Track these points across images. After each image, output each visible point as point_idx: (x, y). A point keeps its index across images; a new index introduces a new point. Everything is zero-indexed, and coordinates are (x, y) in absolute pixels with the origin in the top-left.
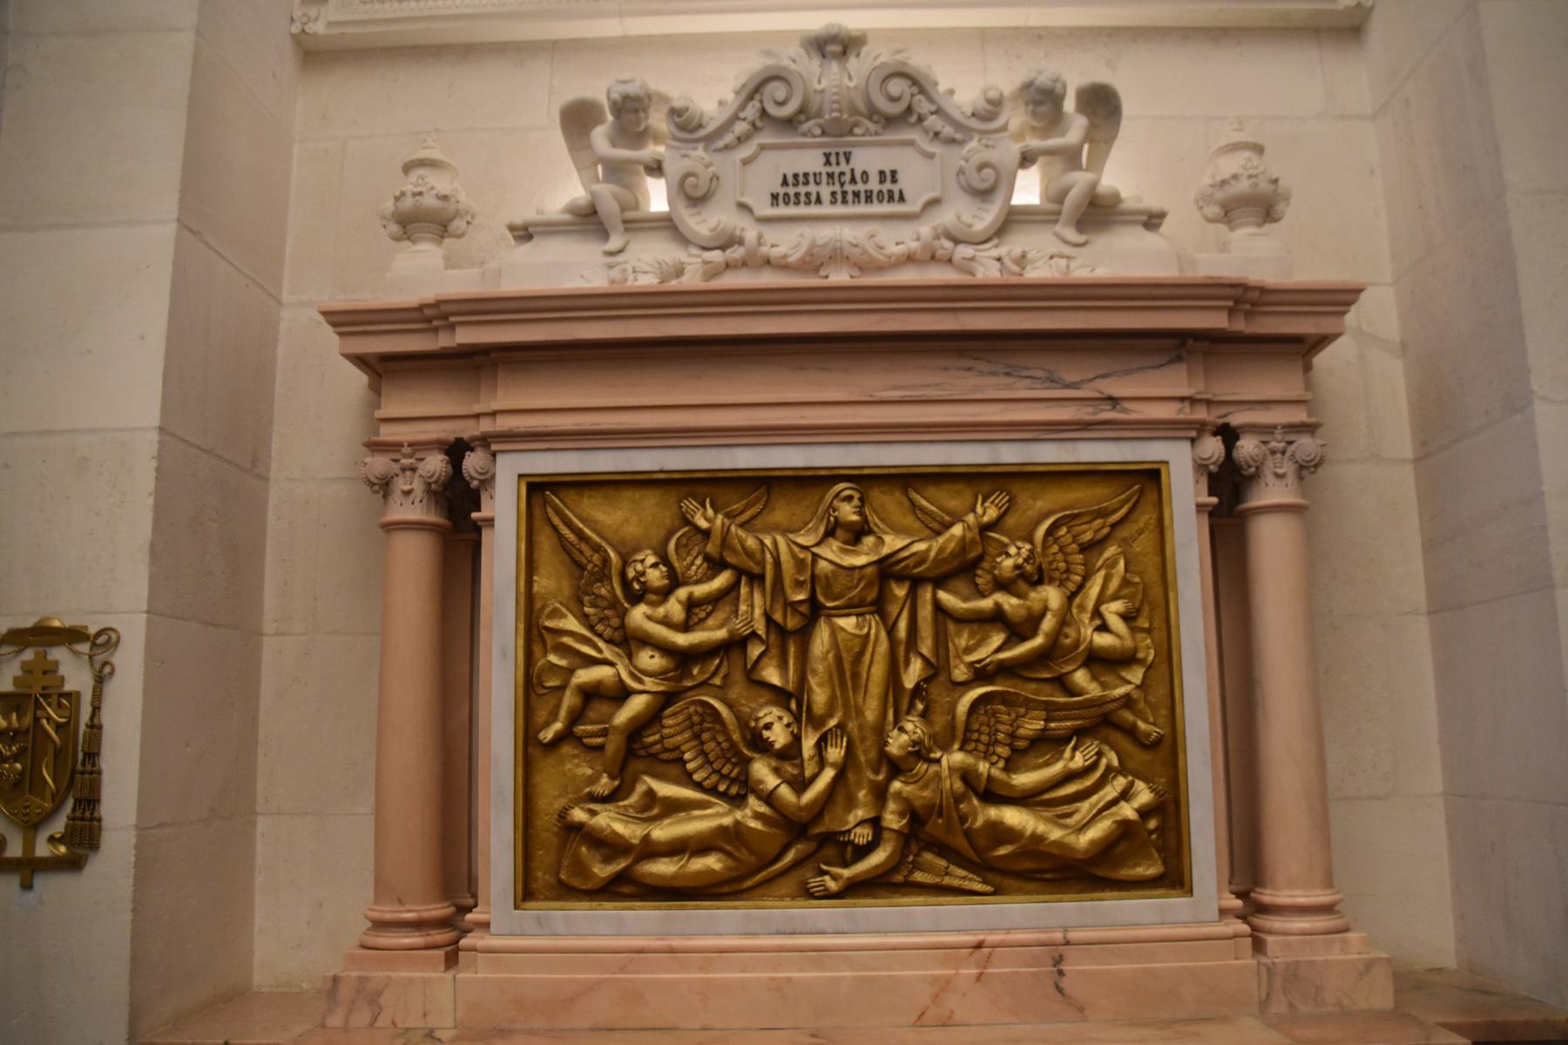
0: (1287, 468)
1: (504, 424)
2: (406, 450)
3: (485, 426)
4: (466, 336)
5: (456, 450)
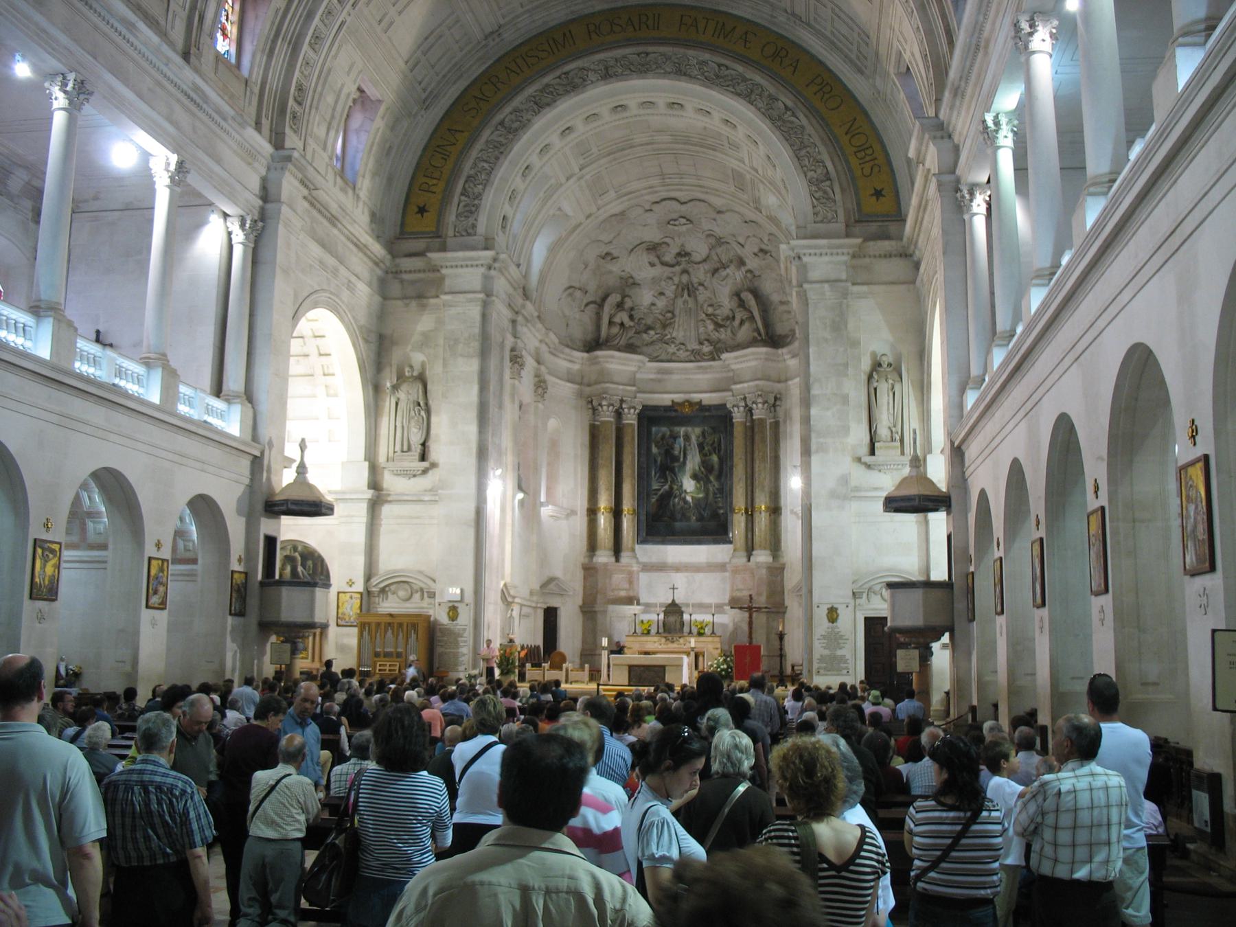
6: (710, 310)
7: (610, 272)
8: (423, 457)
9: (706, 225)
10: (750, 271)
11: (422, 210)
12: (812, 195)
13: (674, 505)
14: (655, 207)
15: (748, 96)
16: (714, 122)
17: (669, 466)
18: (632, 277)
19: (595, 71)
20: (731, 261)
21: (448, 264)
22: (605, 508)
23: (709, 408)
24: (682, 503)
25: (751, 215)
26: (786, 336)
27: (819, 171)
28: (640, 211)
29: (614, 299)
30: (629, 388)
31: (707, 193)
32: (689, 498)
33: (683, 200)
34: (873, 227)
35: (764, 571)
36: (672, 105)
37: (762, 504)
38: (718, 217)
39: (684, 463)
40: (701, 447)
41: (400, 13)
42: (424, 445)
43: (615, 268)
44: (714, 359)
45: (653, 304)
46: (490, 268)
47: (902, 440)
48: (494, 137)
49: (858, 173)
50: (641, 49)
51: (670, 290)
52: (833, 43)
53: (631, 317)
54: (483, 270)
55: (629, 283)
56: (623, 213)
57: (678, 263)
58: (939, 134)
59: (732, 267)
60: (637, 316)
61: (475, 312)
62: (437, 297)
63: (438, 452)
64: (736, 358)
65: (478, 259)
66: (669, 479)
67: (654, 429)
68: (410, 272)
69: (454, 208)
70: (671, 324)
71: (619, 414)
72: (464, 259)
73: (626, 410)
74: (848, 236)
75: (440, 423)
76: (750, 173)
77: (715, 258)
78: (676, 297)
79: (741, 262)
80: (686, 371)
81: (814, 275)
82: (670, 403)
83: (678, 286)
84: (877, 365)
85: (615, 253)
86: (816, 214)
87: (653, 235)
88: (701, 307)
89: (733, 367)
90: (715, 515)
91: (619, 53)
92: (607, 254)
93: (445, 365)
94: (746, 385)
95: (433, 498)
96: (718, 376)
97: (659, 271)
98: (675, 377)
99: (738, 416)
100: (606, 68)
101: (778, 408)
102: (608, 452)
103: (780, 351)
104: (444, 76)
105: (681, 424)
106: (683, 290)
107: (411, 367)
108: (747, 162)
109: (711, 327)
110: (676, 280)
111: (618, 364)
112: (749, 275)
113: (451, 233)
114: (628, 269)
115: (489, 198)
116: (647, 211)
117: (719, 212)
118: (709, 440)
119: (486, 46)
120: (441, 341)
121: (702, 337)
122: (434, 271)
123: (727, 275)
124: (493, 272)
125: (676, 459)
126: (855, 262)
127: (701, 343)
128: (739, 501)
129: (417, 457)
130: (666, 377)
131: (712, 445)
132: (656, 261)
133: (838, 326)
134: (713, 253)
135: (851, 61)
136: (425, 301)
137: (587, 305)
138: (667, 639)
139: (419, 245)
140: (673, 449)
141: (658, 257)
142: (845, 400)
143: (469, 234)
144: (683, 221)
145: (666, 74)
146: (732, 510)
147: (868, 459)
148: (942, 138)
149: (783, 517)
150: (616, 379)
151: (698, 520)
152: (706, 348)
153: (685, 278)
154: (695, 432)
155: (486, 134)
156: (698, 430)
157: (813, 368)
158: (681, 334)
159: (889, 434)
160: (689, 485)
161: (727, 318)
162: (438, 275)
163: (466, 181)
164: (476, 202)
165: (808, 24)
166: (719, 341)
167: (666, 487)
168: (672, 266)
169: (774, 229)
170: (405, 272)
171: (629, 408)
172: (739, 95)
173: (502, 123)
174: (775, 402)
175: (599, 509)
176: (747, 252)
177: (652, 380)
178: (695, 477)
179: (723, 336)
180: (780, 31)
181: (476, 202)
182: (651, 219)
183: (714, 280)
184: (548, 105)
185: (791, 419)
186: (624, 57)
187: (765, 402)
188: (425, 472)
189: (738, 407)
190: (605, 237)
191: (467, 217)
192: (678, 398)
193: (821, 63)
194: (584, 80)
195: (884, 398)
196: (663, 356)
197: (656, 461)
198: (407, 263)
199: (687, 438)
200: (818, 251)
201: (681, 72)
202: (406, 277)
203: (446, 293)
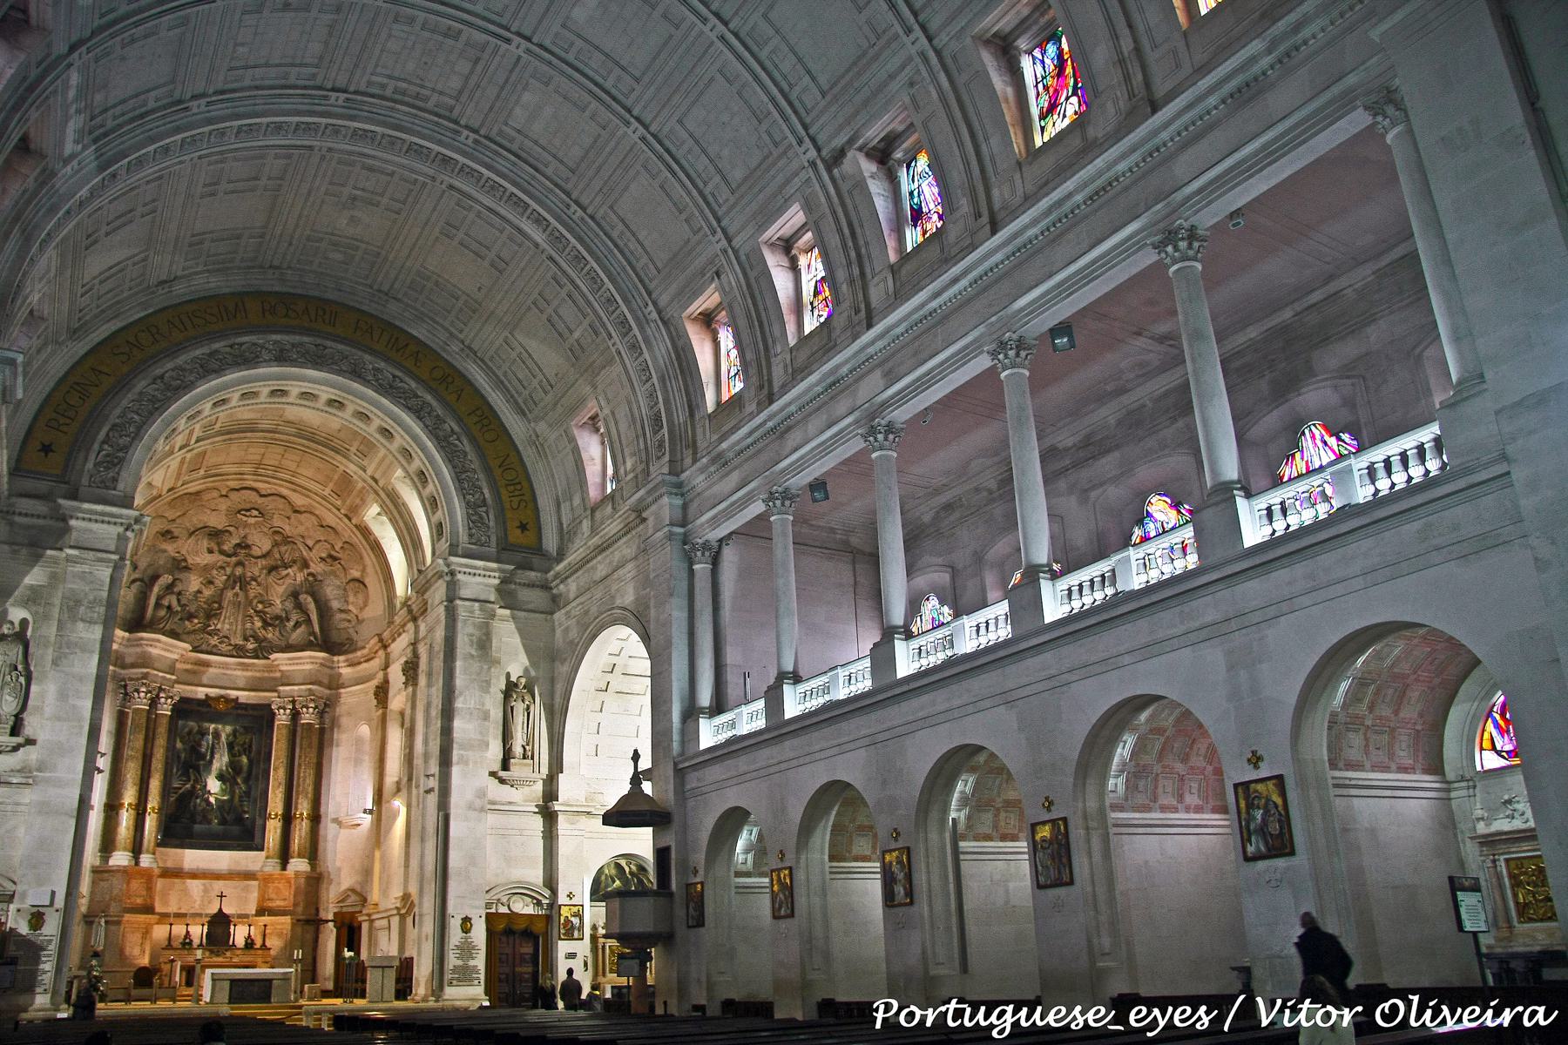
6: (260, 607)
7: (165, 551)
8: (15, 731)
9: (277, 522)
10: (310, 574)
11: (47, 449)
12: (469, 518)
13: (195, 806)
14: (233, 495)
15: (418, 412)
16: (371, 430)
17: (191, 763)
18: (185, 560)
19: (270, 351)
20: (294, 562)
21: (80, 515)
22: (130, 805)
23: (246, 706)
24: (204, 804)
25: (330, 519)
26: (343, 645)
27: (477, 496)
28: (215, 494)
29: (166, 579)
30: (168, 676)
31: (294, 491)
32: (212, 800)
33: (264, 493)
34: (519, 557)
35: (303, 880)
36: (331, 402)
37: (303, 807)
38: (293, 516)
39: (211, 762)
40: (231, 746)
41: (107, 234)
42: (16, 716)
43: (170, 548)
44: (258, 658)
45: (199, 592)
46: (127, 529)
47: (532, 758)
48: (150, 390)
49: (507, 506)
50: (319, 341)
51: (220, 580)
52: (502, 382)
53: (179, 600)
54: (121, 529)
55: (180, 566)
56: (198, 493)
57: (235, 554)
58: (674, 491)
59: (295, 568)
60: (184, 601)
61: (105, 573)
62: (61, 549)
63: (32, 726)
64: (289, 659)
65: (120, 516)
66: (192, 778)
67: (180, 722)
68: (26, 515)
69: (92, 457)
70: (215, 615)
71: (154, 703)
72: (103, 514)
73: (163, 700)
74: (498, 561)
75: (45, 692)
76: (365, 481)
77: (278, 556)
78: (225, 588)
79: (306, 565)
80: (225, 666)
81: (464, 593)
82: (201, 696)
83: (229, 577)
84: (511, 688)
85: (176, 532)
86: (471, 535)
87: (217, 521)
88: (251, 602)
89: (283, 668)
90: (239, 820)
91: (297, 339)
92: (168, 532)
93: (60, 628)
94: (296, 688)
95: (24, 781)
96: (258, 674)
97: (216, 558)
98: (211, 670)
99: (282, 718)
100: (282, 351)
101: (326, 715)
102: (135, 742)
103: (336, 658)
104: (103, 311)
105: (212, 721)
106: (235, 582)
107: (12, 623)
108: (369, 472)
109: (258, 624)
110: (229, 570)
111: (164, 648)
112: (311, 579)
113: (85, 481)
114: (184, 552)
115: (138, 453)
116: (222, 496)
117: (296, 511)
118: (240, 739)
119: (153, 293)
120: (57, 601)
121: (249, 633)
122: (57, 519)
123: (287, 575)
124: (129, 534)
125: (203, 757)
126: (505, 587)
127: (246, 639)
128: (276, 804)
129: (8, 731)
130: (202, 668)
131: (242, 745)
132: (216, 548)
133: (484, 643)
134: (276, 550)
135: (516, 402)
136: (40, 551)
137: (134, 581)
138: (212, 952)
139: (43, 486)
140: (200, 745)
141: (219, 544)
142: (486, 716)
143: (107, 488)
144: (255, 513)
145: (340, 372)
146: (265, 817)
147: (502, 774)
148: (676, 494)
149: (322, 826)
150: (156, 665)
151: (220, 823)
152: (251, 646)
153: (239, 571)
154: (226, 730)
155: (141, 385)
156: (229, 729)
157: (459, 681)
158: (227, 626)
159: (521, 750)
160: (214, 785)
161: (277, 617)
162: (61, 525)
163: (111, 430)
164: (121, 454)
165: (482, 360)
166: (265, 639)
167: (188, 786)
168: (229, 556)
169: (357, 539)
170: (20, 514)
171: (166, 699)
172: (409, 409)
173: (162, 377)
174: (327, 708)
175: (122, 804)
176: (313, 556)
177: (187, 671)
178: (220, 777)
179: (270, 636)
180: (449, 358)
181: (121, 454)
182: (223, 505)
183: (270, 579)
184: (215, 371)
185: (339, 727)
186: (301, 344)
187: (316, 707)
188: (16, 749)
189: (285, 709)
190: (170, 514)
191: (107, 469)
192: (213, 692)
193: (483, 397)
194: (257, 357)
195: (519, 718)
196: (204, 647)
197: (179, 757)
198: (25, 504)
199: (217, 735)
200: (473, 571)
201: (356, 373)
202: (17, 519)
203: (71, 547)
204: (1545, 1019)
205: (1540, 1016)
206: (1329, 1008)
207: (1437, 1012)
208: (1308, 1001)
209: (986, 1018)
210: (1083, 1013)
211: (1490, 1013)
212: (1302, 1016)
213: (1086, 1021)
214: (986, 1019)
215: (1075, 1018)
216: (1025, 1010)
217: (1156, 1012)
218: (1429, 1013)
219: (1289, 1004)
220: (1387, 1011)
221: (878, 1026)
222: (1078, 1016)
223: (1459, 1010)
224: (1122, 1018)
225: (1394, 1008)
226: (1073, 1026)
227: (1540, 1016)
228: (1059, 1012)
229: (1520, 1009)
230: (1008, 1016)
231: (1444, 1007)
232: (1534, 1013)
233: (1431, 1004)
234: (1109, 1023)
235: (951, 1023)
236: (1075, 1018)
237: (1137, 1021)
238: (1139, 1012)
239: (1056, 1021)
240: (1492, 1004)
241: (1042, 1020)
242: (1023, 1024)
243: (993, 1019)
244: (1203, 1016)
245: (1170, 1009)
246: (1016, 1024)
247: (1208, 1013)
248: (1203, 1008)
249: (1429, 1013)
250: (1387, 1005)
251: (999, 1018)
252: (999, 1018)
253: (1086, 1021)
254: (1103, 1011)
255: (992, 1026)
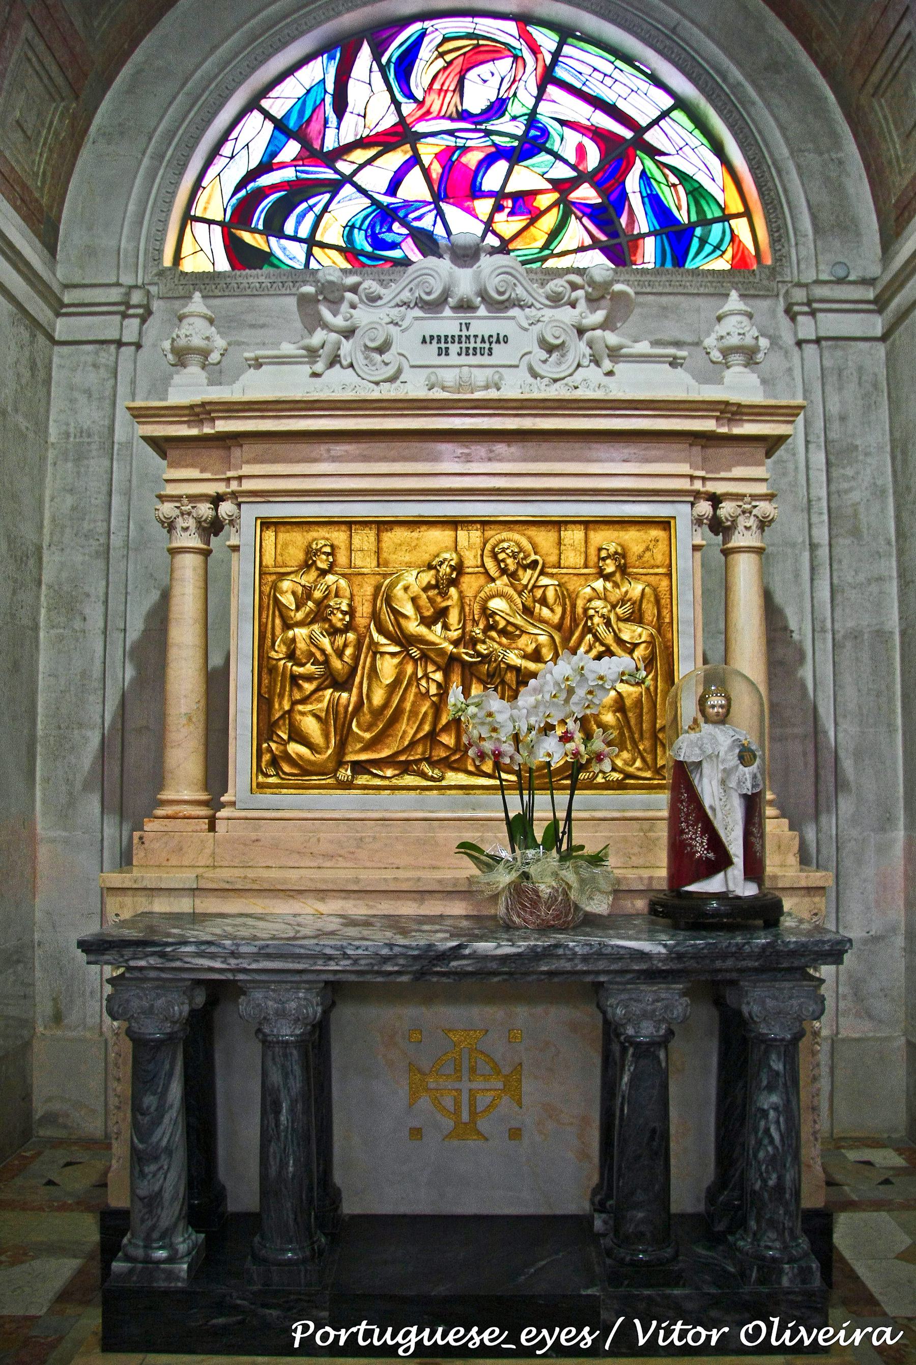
0: (752, 522)
1: (248, 485)
2: (185, 501)
3: (234, 486)
4: (223, 426)
5: (217, 500)
204: (892, 1339)
205: (887, 1336)
206: (699, 1329)
207: (795, 1332)
208: (680, 1322)
209: (393, 1338)
210: (479, 1333)
211: (842, 1333)
212: (675, 1336)
213: (482, 1340)
214: (392, 1339)
215: (472, 1338)
216: (427, 1331)
217: (545, 1332)
218: (788, 1333)
219: (663, 1325)
220: (750, 1331)
221: (296, 1345)
222: (475, 1336)
223: (815, 1331)
224: (514, 1338)
225: (757, 1329)
226: (470, 1345)
227: (887, 1336)
228: (457, 1332)
229: (870, 1329)
230: (412, 1336)
231: (802, 1328)
232: (881, 1334)
233: (790, 1325)
234: (503, 1342)
235: (361, 1343)
236: (472, 1338)
237: (528, 1340)
238: (530, 1332)
239: (456, 1340)
240: (845, 1325)
241: (443, 1339)
242: (426, 1343)
243: (399, 1338)
244: (587, 1336)
245: (557, 1330)
246: (419, 1343)
247: (590, 1333)
248: (587, 1329)
249: (788, 1333)
250: (751, 1326)
251: (404, 1338)
252: (404, 1338)
253: (482, 1340)
254: (497, 1331)
255: (398, 1345)
